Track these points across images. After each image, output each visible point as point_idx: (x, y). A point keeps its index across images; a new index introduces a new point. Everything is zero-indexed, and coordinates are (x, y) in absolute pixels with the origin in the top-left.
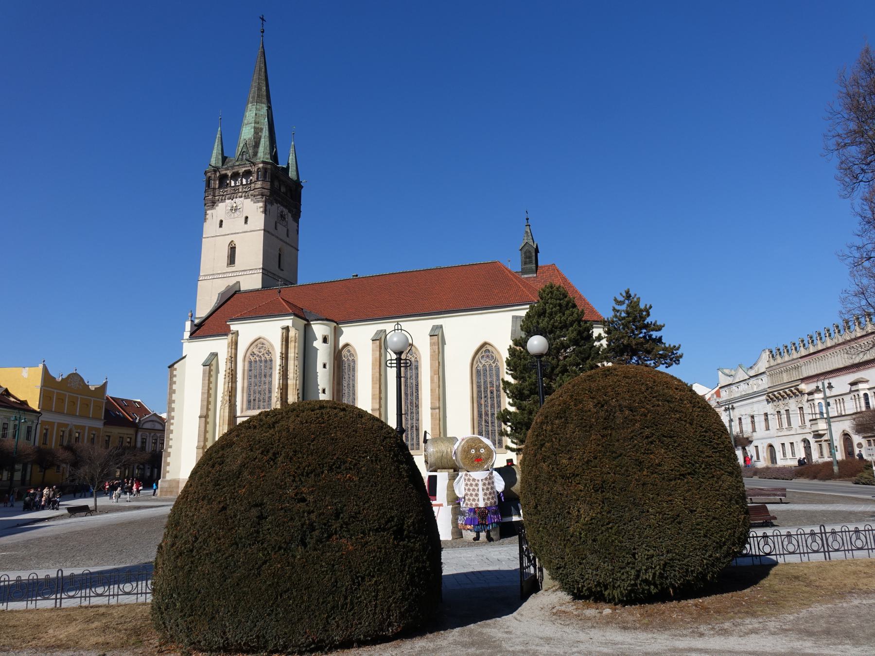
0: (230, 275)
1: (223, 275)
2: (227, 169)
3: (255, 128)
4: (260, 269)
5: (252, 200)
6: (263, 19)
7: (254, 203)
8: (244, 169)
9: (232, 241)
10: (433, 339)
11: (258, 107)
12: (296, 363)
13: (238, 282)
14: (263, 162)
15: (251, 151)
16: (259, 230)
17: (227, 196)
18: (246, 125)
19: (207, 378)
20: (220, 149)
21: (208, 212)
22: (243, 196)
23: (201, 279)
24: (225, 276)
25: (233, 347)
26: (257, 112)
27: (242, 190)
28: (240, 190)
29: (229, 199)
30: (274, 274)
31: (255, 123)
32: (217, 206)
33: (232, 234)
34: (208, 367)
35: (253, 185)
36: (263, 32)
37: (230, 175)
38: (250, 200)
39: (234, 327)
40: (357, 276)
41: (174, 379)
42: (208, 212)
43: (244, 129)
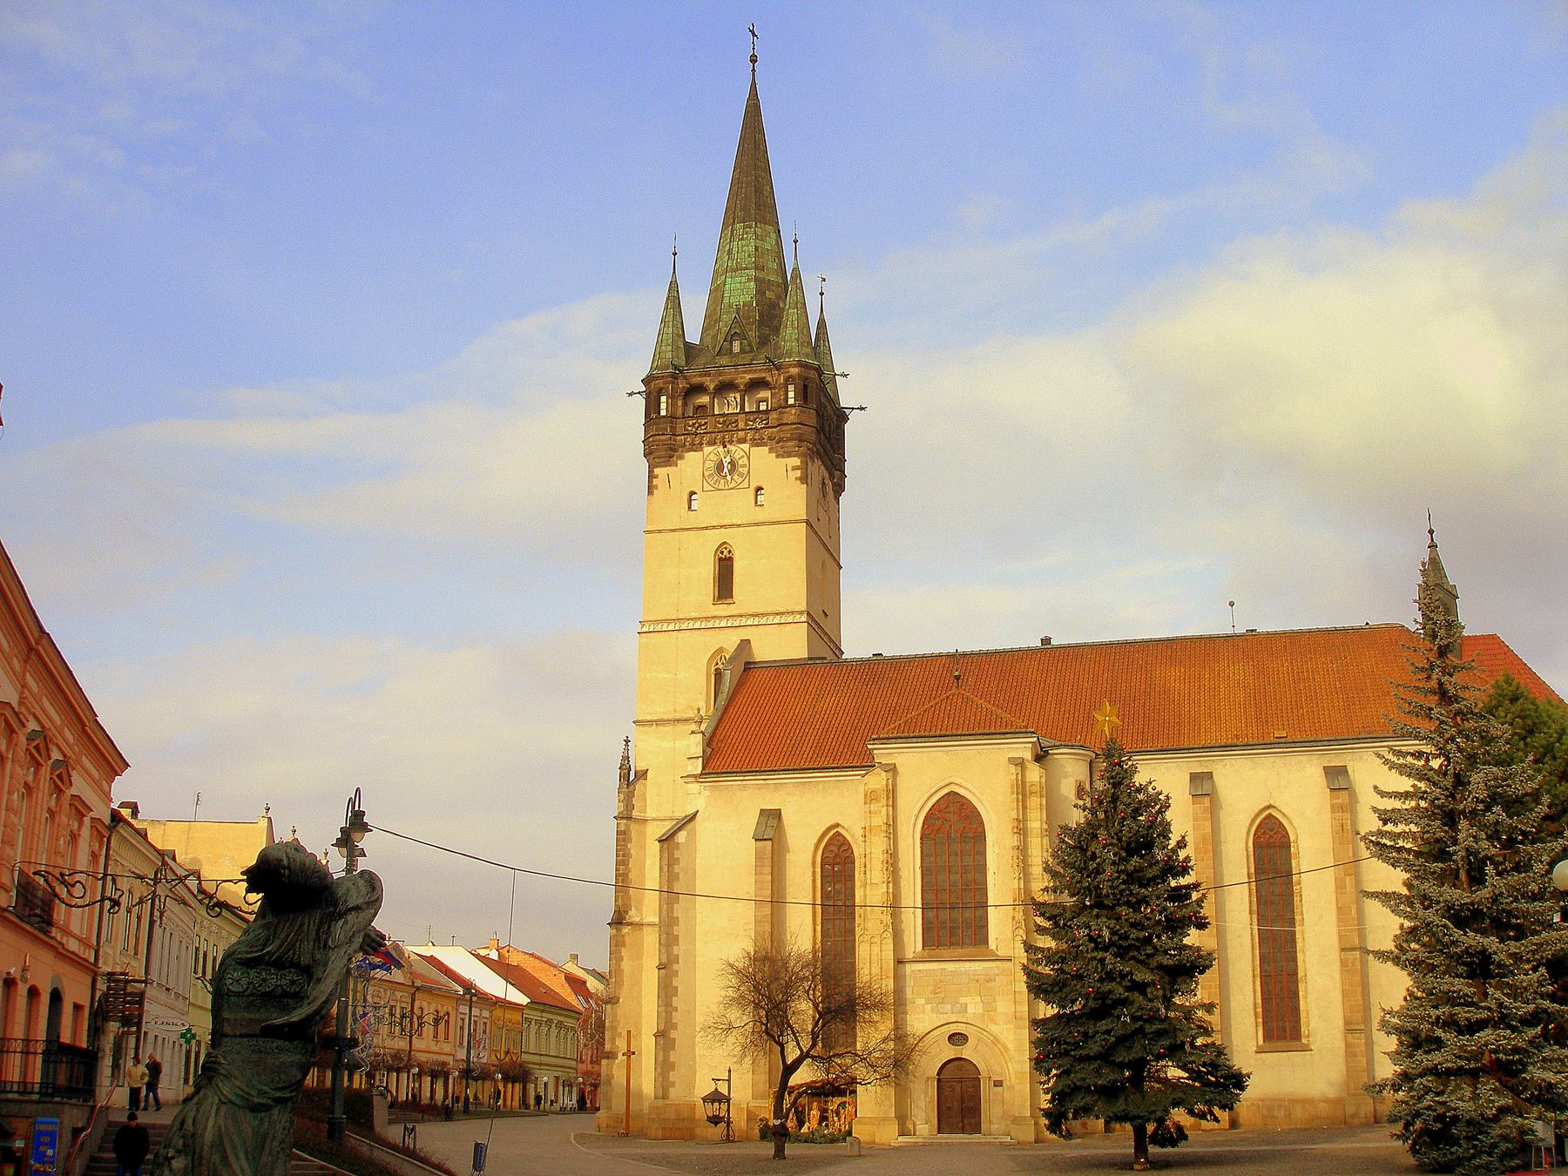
0: (723, 624)
1: (703, 623)
2: (707, 374)
3: (757, 279)
4: (801, 613)
5: (771, 451)
6: (754, 35)
7: (777, 457)
8: (750, 376)
9: (725, 543)
10: (1338, 798)
11: (759, 231)
12: (1046, 841)
13: (745, 644)
14: (800, 364)
15: (753, 334)
16: (797, 522)
17: (706, 439)
18: (733, 270)
19: (768, 870)
20: (679, 325)
21: (657, 471)
22: (748, 438)
23: (645, 629)
24: (710, 625)
25: (891, 803)
26: (759, 243)
27: (747, 425)
28: (742, 424)
29: (710, 444)
30: (820, 627)
31: (759, 267)
32: (681, 458)
33: (722, 527)
34: (770, 842)
35: (774, 415)
36: (754, 60)
37: (712, 387)
38: (766, 449)
39: (883, 753)
40: (1046, 641)
41: (677, 869)
42: (657, 471)
43: (728, 280)
